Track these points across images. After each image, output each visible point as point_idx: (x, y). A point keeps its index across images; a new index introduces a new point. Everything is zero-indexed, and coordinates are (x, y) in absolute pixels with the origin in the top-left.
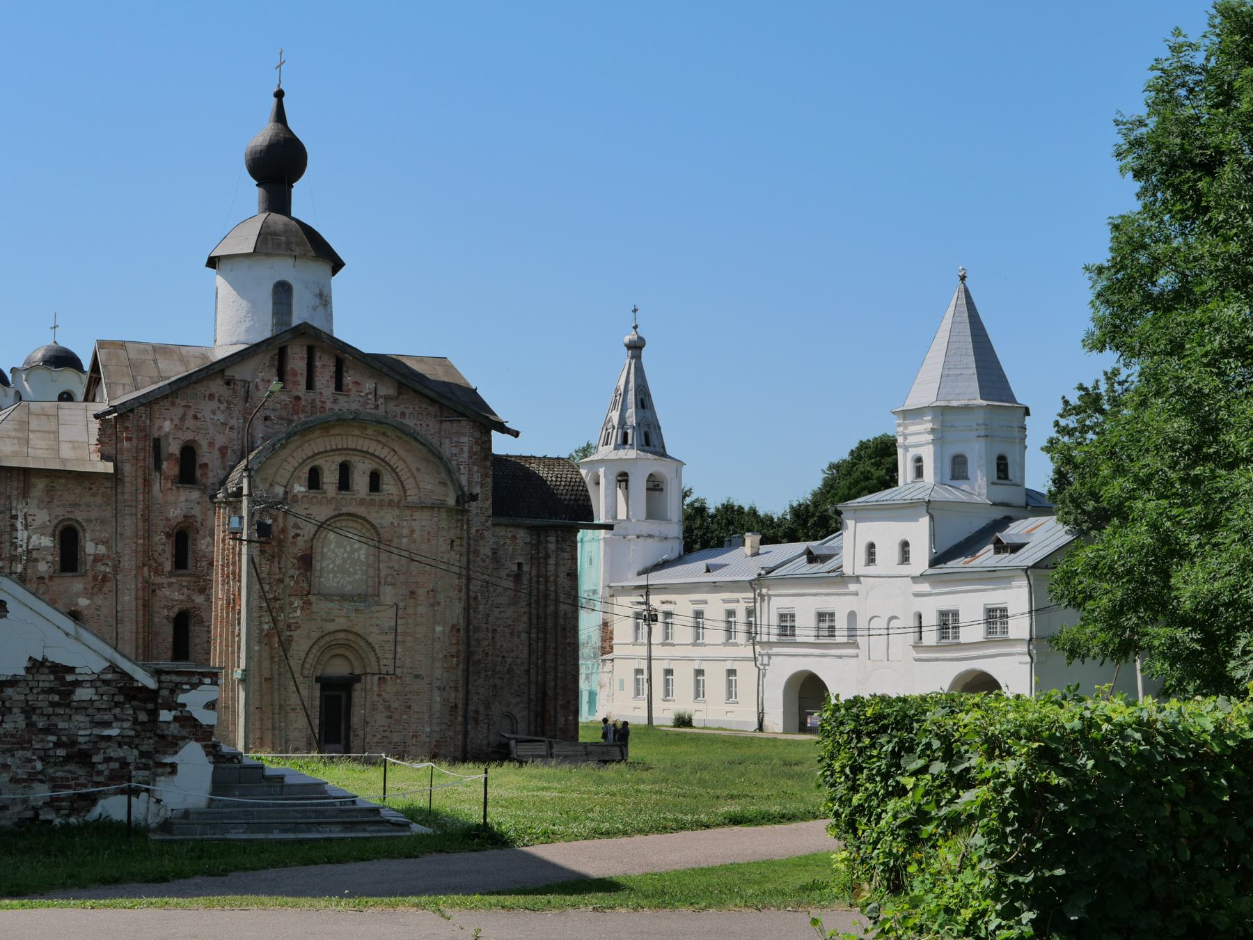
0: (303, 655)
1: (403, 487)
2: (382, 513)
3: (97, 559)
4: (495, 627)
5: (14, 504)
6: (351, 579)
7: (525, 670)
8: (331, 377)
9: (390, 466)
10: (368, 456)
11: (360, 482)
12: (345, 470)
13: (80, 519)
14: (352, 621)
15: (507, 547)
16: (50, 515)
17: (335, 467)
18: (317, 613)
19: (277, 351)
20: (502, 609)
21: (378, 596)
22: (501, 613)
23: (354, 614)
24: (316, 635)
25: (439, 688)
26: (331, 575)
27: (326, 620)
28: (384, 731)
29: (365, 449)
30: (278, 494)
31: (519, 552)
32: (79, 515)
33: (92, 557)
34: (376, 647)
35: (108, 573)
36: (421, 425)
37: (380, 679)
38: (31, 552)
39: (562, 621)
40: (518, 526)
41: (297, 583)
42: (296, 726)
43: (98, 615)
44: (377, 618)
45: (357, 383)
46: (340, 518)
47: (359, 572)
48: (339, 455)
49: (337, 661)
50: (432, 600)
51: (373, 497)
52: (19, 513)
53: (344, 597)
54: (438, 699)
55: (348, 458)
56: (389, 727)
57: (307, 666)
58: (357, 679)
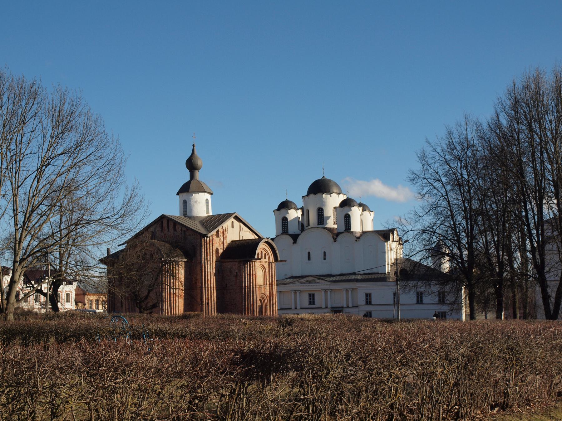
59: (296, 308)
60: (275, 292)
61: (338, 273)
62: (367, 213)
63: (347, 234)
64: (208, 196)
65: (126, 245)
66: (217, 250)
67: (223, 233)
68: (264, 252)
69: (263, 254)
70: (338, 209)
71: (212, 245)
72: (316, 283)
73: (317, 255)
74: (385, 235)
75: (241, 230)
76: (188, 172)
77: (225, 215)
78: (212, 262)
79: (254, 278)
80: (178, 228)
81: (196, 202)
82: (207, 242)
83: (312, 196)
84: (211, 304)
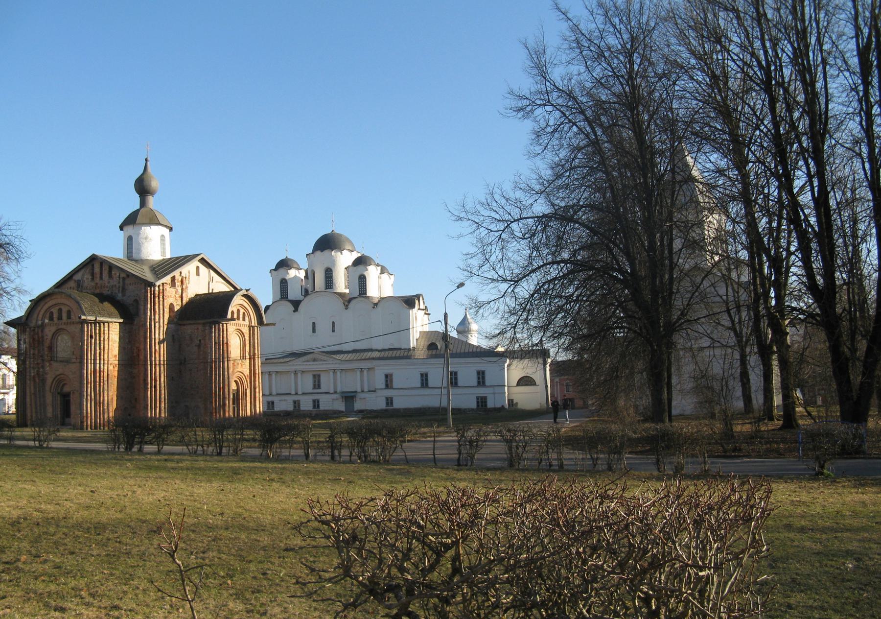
11: (64, 316)
12: (60, 310)
24: (54, 376)
40: (199, 324)
59: (296, 394)
60: (258, 370)
61: (350, 350)
62: (385, 276)
63: (363, 299)
64: (165, 231)
66: (171, 306)
67: (182, 282)
68: (242, 311)
69: (241, 314)
70: (351, 269)
71: (163, 299)
72: (321, 360)
73: (324, 327)
74: (410, 302)
75: (211, 280)
76: (136, 198)
77: (186, 257)
78: (162, 324)
79: (225, 349)
81: (146, 238)
82: (154, 294)
83: (318, 253)
84: (160, 387)
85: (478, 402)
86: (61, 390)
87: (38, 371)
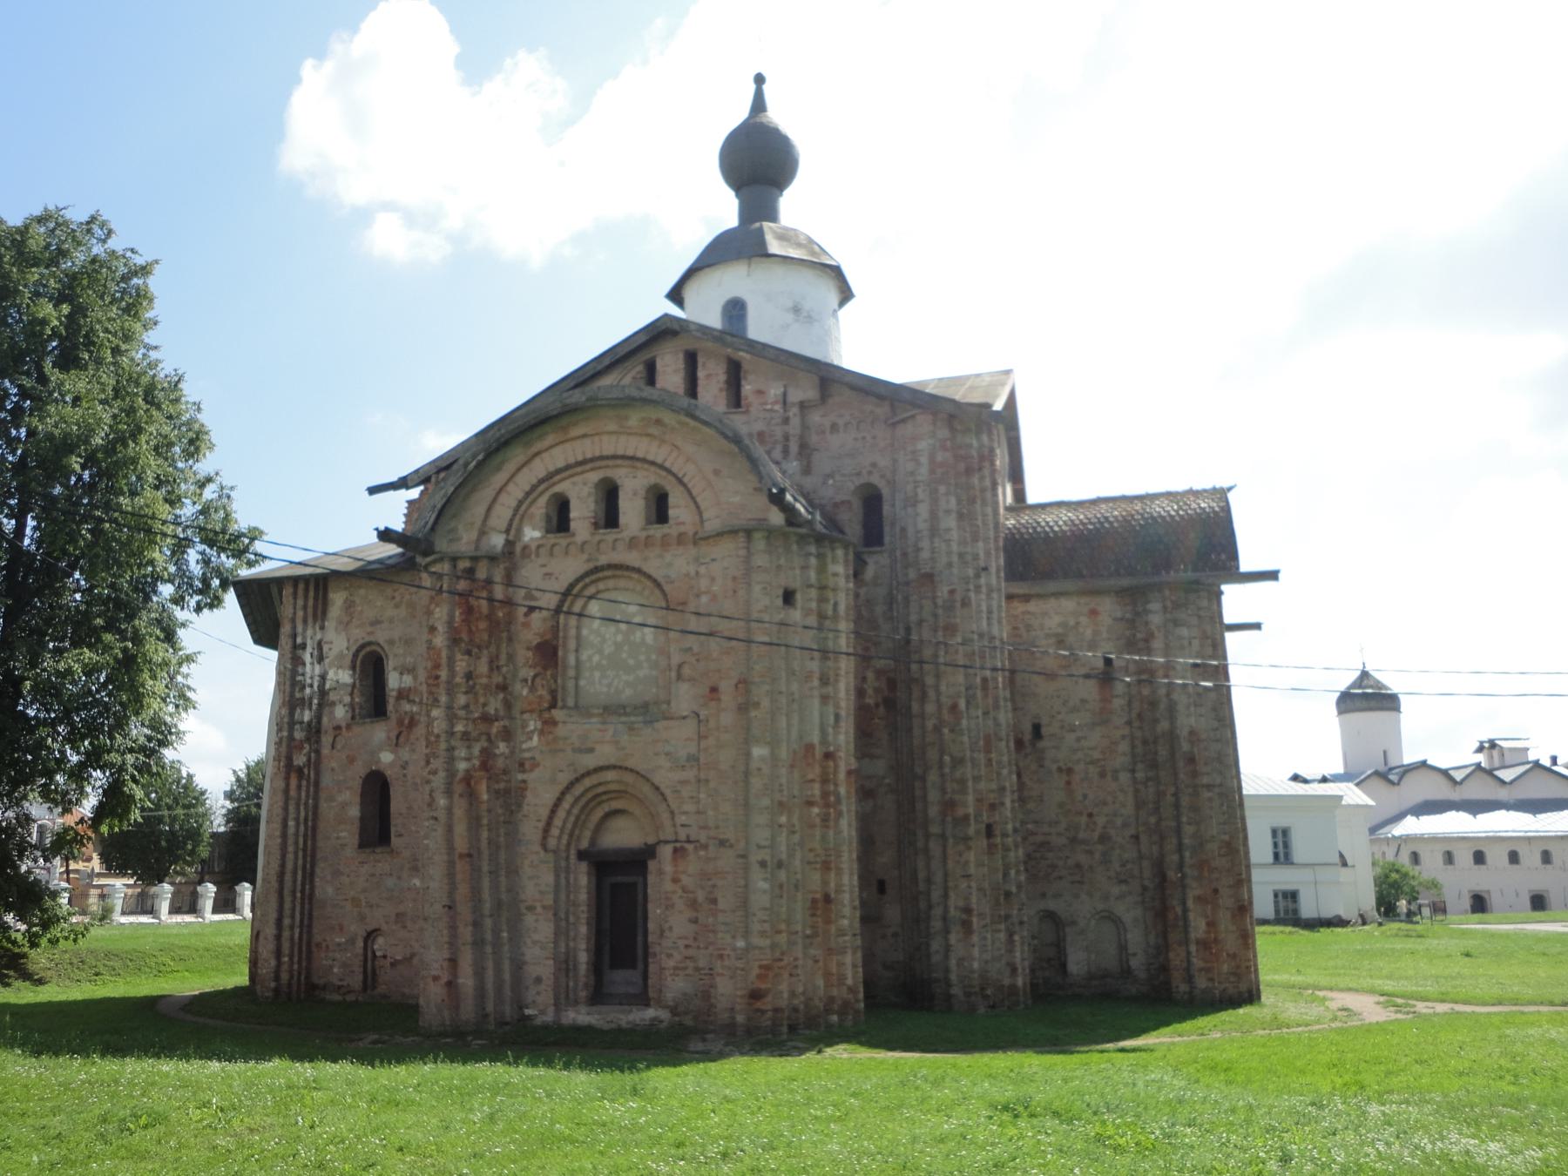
0: (544, 813)
1: (698, 507)
2: (668, 557)
3: (403, 695)
4: (1070, 765)
5: (300, 629)
6: (631, 678)
7: (1132, 836)
8: (721, 390)
9: (674, 475)
10: (639, 464)
11: (632, 510)
12: (610, 495)
13: (381, 642)
14: (623, 749)
15: (1081, 630)
16: (348, 640)
17: (586, 490)
18: (566, 738)
19: (640, 368)
20: (1079, 734)
21: (669, 703)
22: (1078, 740)
23: (626, 737)
24: (564, 778)
25: (763, 864)
26: (597, 674)
27: (580, 751)
28: (687, 946)
29: (630, 452)
30: (495, 547)
31: (1105, 635)
32: (381, 636)
33: (394, 694)
34: (668, 792)
35: (416, 713)
36: (864, 438)
37: (676, 850)
38: (328, 693)
39: (1185, 747)
41: (533, 689)
42: (536, 937)
43: (405, 776)
44: (666, 741)
45: (760, 392)
46: (600, 575)
47: (645, 665)
48: (592, 469)
49: (619, 823)
50: (740, 700)
51: (651, 532)
52: (309, 642)
53: (612, 710)
54: (764, 885)
55: (609, 473)
56: (695, 939)
57: (555, 832)
58: (649, 852)
65: (415, 493)
80: (760, 392)
85: (1276, 903)
86: (593, 841)
87: (487, 755)
